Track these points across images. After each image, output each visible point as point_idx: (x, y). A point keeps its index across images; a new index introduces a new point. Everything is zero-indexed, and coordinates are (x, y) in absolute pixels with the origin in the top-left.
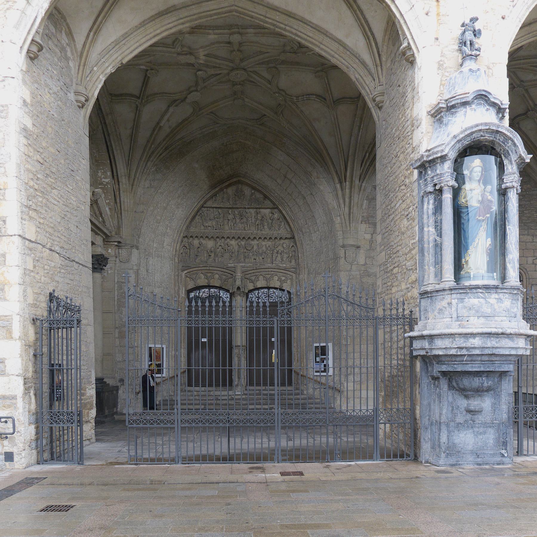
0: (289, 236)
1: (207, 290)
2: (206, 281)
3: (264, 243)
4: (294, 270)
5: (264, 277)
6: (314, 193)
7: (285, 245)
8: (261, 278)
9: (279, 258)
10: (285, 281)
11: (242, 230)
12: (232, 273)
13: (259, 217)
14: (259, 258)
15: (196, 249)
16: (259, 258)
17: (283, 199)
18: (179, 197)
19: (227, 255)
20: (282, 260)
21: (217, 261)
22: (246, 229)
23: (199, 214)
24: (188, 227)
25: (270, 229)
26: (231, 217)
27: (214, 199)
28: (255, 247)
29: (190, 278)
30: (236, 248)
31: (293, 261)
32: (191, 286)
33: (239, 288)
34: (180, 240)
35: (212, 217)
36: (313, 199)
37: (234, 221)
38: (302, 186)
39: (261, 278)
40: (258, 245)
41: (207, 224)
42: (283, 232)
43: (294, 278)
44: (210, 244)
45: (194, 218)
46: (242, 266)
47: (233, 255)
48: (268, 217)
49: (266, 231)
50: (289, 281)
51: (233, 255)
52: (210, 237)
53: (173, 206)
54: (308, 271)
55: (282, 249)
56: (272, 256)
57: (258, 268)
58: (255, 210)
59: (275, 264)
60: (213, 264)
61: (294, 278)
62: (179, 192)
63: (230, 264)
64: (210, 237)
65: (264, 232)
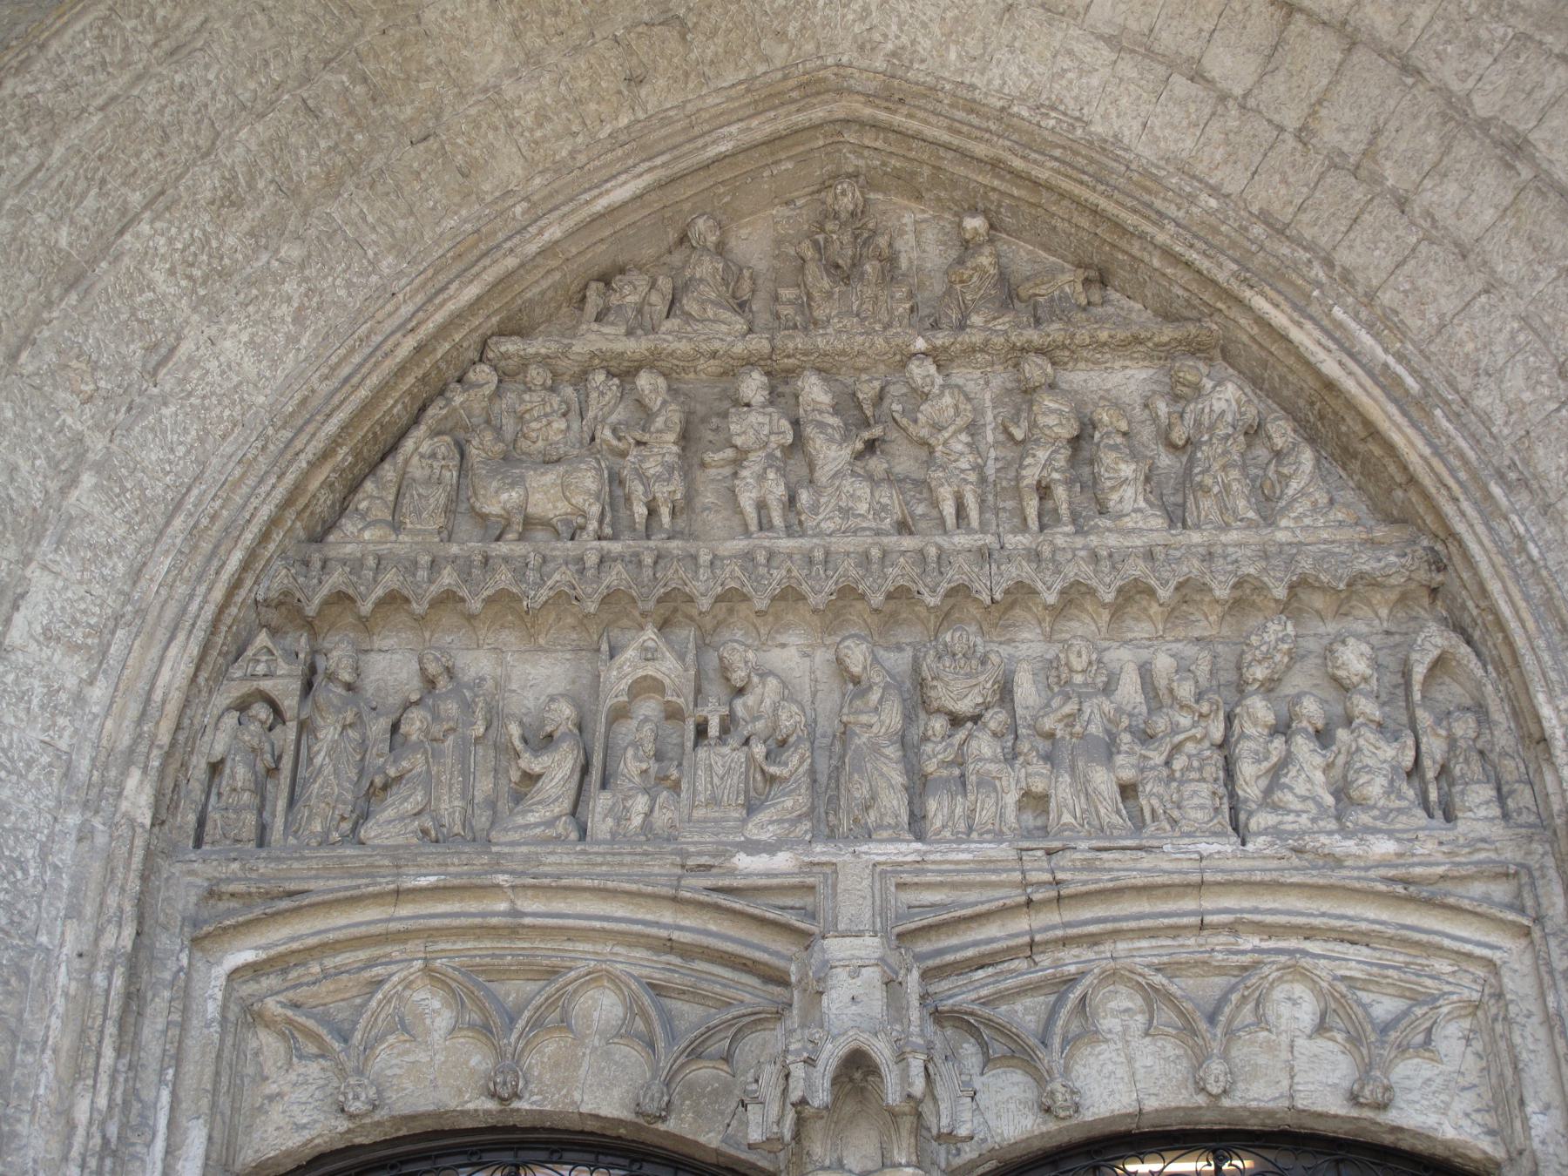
2: (479, 1060)
3: (1122, 657)
5: (1153, 996)
7: (1354, 660)
9: (1310, 772)
11: (878, 533)
13: (1055, 418)
14: (1083, 787)
16: (1083, 787)
17: (1280, 231)
18: (229, 201)
19: (720, 765)
21: (601, 826)
25: (1176, 517)
26: (757, 426)
27: (594, 301)
29: (289, 1033)
31: (1477, 799)
37: (797, 466)
38: (1475, 44)
39: (1118, 1010)
41: (512, 496)
43: (1518, 983)
44: (537, 678)
46: (881, 872)
48: (1146, 433)
50: (1450, 1038)
53: (158, 277)
57: (1076, 881)
59: (1276, 832)
60: (558, 860)
61: (1518, 983)
63: (753, 848)
65: (1113, 540)
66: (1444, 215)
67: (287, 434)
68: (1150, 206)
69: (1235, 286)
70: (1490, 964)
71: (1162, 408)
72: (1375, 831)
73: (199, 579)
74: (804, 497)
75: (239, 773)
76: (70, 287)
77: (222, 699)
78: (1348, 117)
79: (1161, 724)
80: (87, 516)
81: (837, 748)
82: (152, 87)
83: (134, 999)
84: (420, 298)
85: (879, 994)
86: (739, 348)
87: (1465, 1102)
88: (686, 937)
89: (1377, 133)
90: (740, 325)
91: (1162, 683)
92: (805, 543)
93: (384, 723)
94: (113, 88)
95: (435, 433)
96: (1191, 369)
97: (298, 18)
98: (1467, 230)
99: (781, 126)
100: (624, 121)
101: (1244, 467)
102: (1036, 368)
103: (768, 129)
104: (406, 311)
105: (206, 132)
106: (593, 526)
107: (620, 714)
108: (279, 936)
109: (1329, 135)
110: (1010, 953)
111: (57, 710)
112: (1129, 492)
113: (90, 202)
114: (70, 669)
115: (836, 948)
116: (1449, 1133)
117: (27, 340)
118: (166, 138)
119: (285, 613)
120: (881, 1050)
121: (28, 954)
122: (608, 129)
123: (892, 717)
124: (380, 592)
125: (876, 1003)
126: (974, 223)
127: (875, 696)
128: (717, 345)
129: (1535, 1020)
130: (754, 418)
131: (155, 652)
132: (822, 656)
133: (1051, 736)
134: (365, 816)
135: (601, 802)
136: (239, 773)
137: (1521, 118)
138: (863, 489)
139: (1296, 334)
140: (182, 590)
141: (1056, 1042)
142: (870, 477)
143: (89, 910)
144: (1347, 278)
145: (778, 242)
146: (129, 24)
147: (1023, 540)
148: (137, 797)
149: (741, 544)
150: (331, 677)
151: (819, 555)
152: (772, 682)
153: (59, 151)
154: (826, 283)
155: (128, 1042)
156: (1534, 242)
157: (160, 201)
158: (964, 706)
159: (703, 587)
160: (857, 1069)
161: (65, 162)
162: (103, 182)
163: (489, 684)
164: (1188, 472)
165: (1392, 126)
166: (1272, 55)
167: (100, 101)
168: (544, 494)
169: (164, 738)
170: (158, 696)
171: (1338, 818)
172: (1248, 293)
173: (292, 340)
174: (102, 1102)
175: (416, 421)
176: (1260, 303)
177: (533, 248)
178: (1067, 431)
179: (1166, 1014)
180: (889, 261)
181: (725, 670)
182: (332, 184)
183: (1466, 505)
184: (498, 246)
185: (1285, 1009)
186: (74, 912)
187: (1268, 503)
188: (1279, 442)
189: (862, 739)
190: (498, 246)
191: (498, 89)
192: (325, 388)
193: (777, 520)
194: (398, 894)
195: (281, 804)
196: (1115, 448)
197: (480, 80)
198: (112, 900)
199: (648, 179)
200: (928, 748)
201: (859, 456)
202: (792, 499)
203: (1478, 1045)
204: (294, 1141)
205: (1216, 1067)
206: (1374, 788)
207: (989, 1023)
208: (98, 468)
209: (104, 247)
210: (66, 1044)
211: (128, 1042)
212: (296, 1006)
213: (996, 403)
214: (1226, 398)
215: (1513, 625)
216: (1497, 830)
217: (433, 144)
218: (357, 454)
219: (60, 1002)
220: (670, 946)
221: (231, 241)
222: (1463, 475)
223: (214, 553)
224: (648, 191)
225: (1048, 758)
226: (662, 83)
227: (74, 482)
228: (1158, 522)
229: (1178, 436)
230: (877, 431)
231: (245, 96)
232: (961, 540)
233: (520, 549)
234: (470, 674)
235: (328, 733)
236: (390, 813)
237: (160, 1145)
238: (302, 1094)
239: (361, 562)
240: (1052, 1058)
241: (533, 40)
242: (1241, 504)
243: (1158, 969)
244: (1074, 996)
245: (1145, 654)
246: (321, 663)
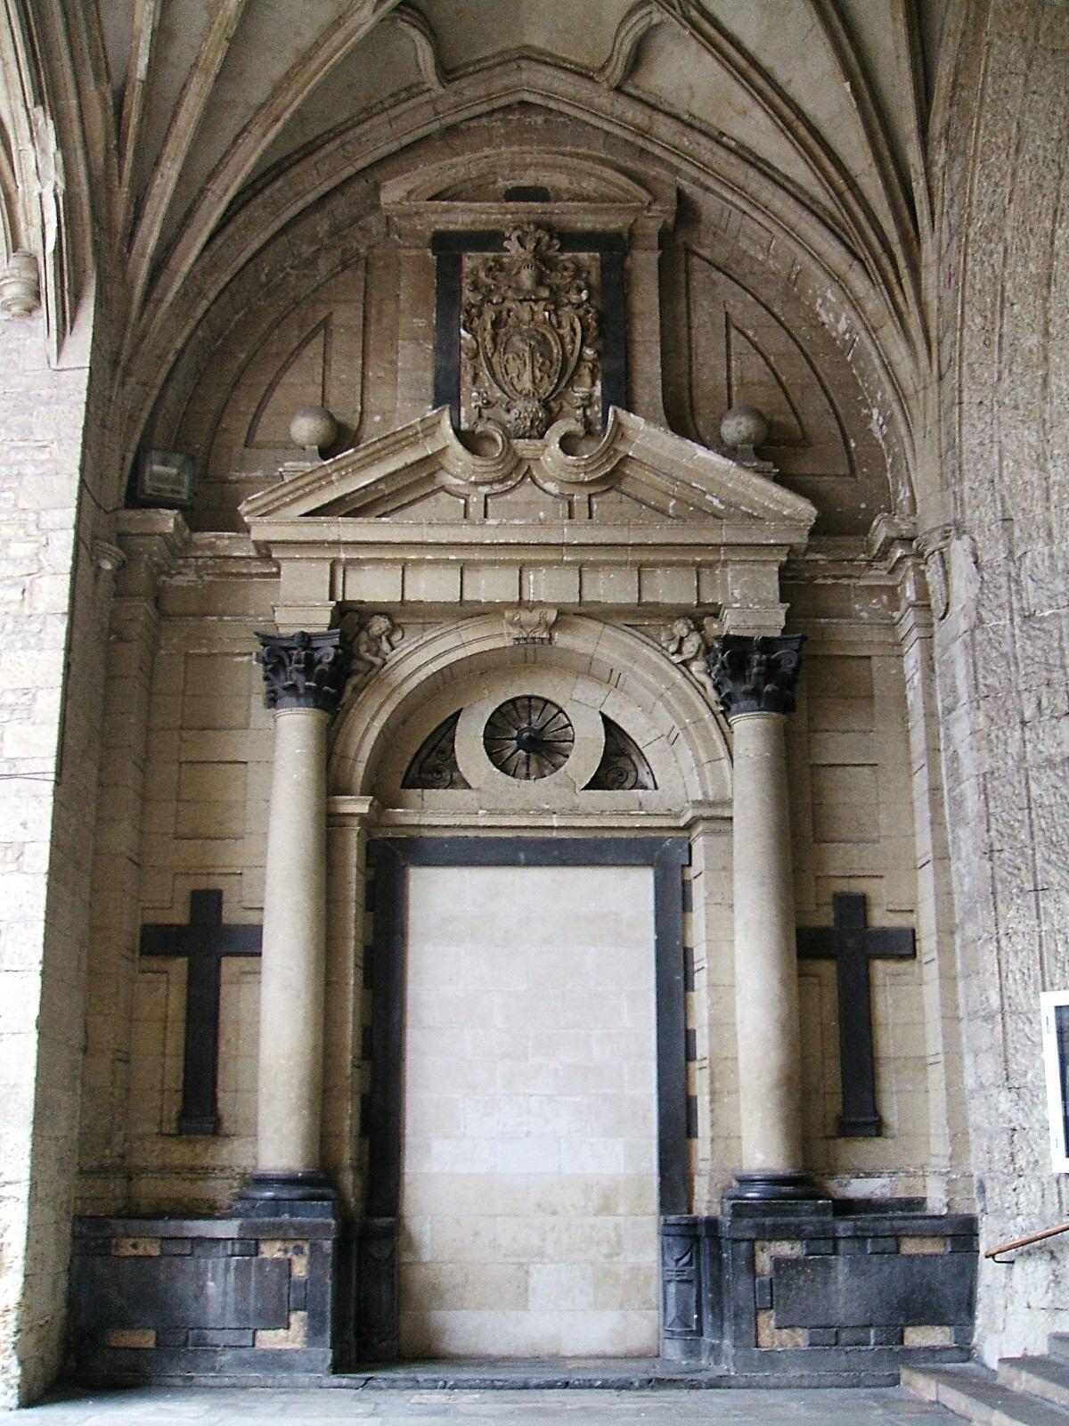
82: (1020, 173)
105: (1054, 167)
117: (1047, 322)
118: (1040, 186)
153: (1008, 235)
161: (1013, 237)
162: (1031, 230)
167: (1007, 200)
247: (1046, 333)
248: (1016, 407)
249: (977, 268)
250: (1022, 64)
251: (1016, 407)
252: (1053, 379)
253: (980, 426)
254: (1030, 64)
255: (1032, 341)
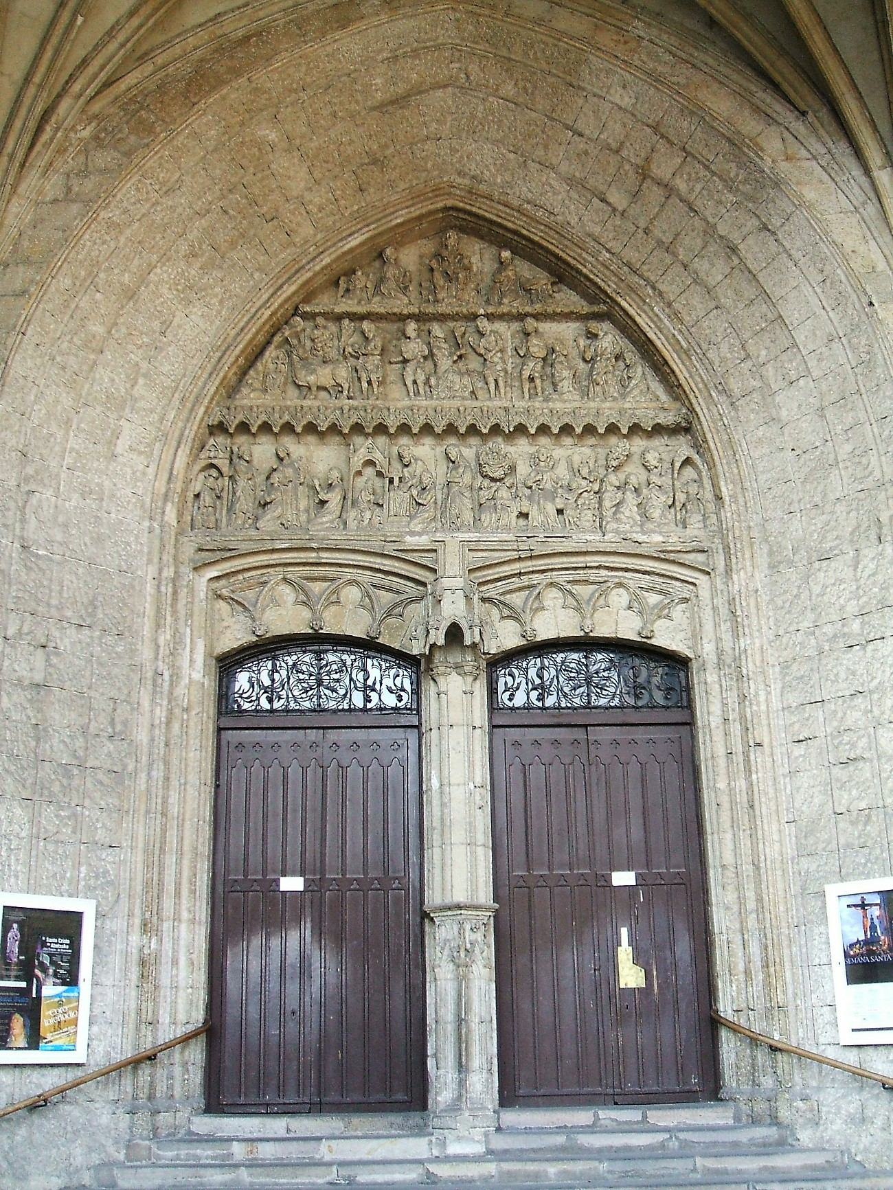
0: (667, 419)
1: (307, 658)
2: (306, 614)
3: (558, 453)
4: (701, 557)
6: (776, 222)
7: (652, 458)
8: (552, 598)
10: (663, 612)
12: (416, 576)
13: (536, 347)
14: (542, 510)
15: (260, 479)
16: (542, 510)
19: (398, 500)
20: (646, 517)
21: (352, 524)
22: (480, 394)
23: (278, 339)
24: (232, 390)
25: (585, 394)
26: (415, 348)
28: (523, 469)
30: (440, 472)
31: (695, 519)
32: (235, 635)
33: (454, 633)
34: (190, 434)
35: (333, 354)
36: (773, 247)
37: (429, 365)
38: (720, 202)
39: (552, 598)
40: (535, 461)
42: (645, 400)
44: (322, 458)
45: (255, 355)
47: (426, 499)
48: (575, 352)
49: (567, 403)
50: (678, 612)
51: (426, 499)
52: (323, 427)
54: (771, 553)
55: (643, 475)
56: (600, 502)
58: (516, 326)
59: (617, 532)
60: (337, 538)
61: (704, 593)
62: (193, 235)
63: (412, 534)
64: (323, 427)
65: (558, 405)
66: (702, 275)
67: (219, 354)
68: (580, 255)
69: (614, 295)
70: (695, 585)
71: (582, 342)
72: (654, 532)
73: (188, 421)
74: (433, 381)
75: (207, 498)
76: (131, 298)
77: (197, 467)
78: (665, 227)
79: (574, 486)
80: (143, 397)
81: (445, 490)
83: (175, 593)
84: (271, 291)
85: (463, 601)
86: (405, 312)
87: (682, 635)
88: (386, 568)
89: (678, 234)
90: (406, 300)
91: (576, 466)
92: (434, 403)
93: (264, 477)
94: (144, 211)
95: (277, 348)
96: (594, 326)
97: (218, 171)
98: (712, 282)
99: (424, 211)
100: (356, 207)
101: (614, 375)
102: (531, 323)
103: (418, 213)
104: (265, 297)
106: (345, 393)
107: (359, 473)
108: (227, 567)
109: (657, 233)
110: (513, 576)
111: (137, 480)
112: (565, 383)
113: (136, 262)
114: (139, 462)
115: (446, 583)
116: (674, 648)
119: (219, 428)
120: (464, 625)
121: (134, 579)
122: (349, 211)
123: (467, 479)
124: (259, 422)
125: (461, 603)
126: (506, 254)
127: (461, 471)
128: (395, 310)
129: (710, 606)
130: (412, 345)
131: (172, 451)
132: (440, 450)
133: (530, 487)
134: (257, 519)
135: (352, 514)
136: (207, 498)
137: (735, 237)
138: (457, 378)
139: (638, 319)
140: (180, 424)
141: (528, 611)
142: (461, 374)
143: (156, 560)
144: (661, 294)
145: (421, 257)
146: (148, 182)
147: (523, 404)
148: (171, 515)
149: (407, 403)
150: (240, 457)
151: (439, 409)
152: (419, 463)
153: (122, 240)
154: (442, 283)
155: (175, 612)
156: (736, 292)
157: (165, 258)
158: (496, 475)
159: (392, 424)
160: (454, 633)
161: (126, 245)
163: (304, 460)
164: (590, 374)
165: (684, 233)
166: (635, 195)
168: (323, 375)
169: (179, 490)
170: (175, 472)
171: (641, 526)
172: (619, 299)
173: (219, 312)
174: (168, 637)
175: (269, 343)
176: (623, 303)
177: (317, 268)
178: (543, 354)
179: (571, 601)
180: (468, 268)
181: (400, 457)
182: (233, 245)
183: (700, 400)
184: (303, 267)
185: (616, 598)
186: (149, 562)
187: (623, 385)
188: (628, 362)
189: (455, 489)
190: (303, 267)
191: (302, 196)
192: (233, 333)
193: (421, 391)
194: (273, 551)
195: (224, 512)
196: (561, 363)
197: (295, 193)
198: (165, 558)
199: (367, 235)
200: (482, 493)
201: (455, 362)
202: (428, 380)
203: (687, 614)
204: (236, 645)
205: (588, 622)
206: (656, 513)
207: (502, 603)
208: (145, 376)
209: (143, 280)
210: (152, 613)
211: (175, 612)
212: (233, 592)
213: (513, 337)
214: (609, 338)
215: (715, 452)
216: (701, 533)
217: (275, 222)
218: (246, 359)
219: (148, 598)
220: (379, 571)
221: (193, 272)
222: (701, 385)
223: (192, 410)
224: (367, 239)
225: (530, 498)
226: (372, 190)
227: (136, 383)
228: (577, 397)
229: (588, 356)
230: (463, 351)
231: (197, 209)
232: (497, 403)
233: (316, 403)
234: (294, 456)
235: (242, 483)
236: (268, 517)
237: (188, 649)
238: (237, 626)
239: (251, 408)
240: (526, 617)
241: (317, 174)
242: (612, 389)
243: (569, 582)
244: (535, 593)
245: (570, 452)
246: (235, 449)
247: (109, 332)
248: (63, 368)
249: (88, 243)
250: (211, 145)
251: (63, 368)
252: (100, 369)
253: (30, 363)
254: (215, 150)
255: (98, 329)
